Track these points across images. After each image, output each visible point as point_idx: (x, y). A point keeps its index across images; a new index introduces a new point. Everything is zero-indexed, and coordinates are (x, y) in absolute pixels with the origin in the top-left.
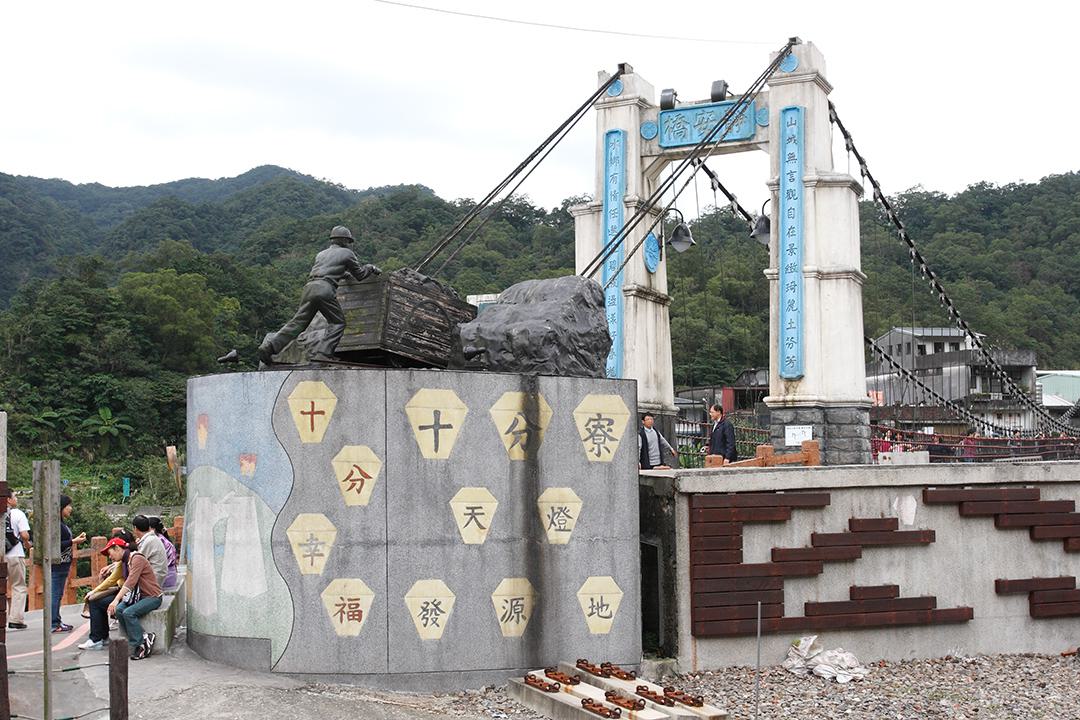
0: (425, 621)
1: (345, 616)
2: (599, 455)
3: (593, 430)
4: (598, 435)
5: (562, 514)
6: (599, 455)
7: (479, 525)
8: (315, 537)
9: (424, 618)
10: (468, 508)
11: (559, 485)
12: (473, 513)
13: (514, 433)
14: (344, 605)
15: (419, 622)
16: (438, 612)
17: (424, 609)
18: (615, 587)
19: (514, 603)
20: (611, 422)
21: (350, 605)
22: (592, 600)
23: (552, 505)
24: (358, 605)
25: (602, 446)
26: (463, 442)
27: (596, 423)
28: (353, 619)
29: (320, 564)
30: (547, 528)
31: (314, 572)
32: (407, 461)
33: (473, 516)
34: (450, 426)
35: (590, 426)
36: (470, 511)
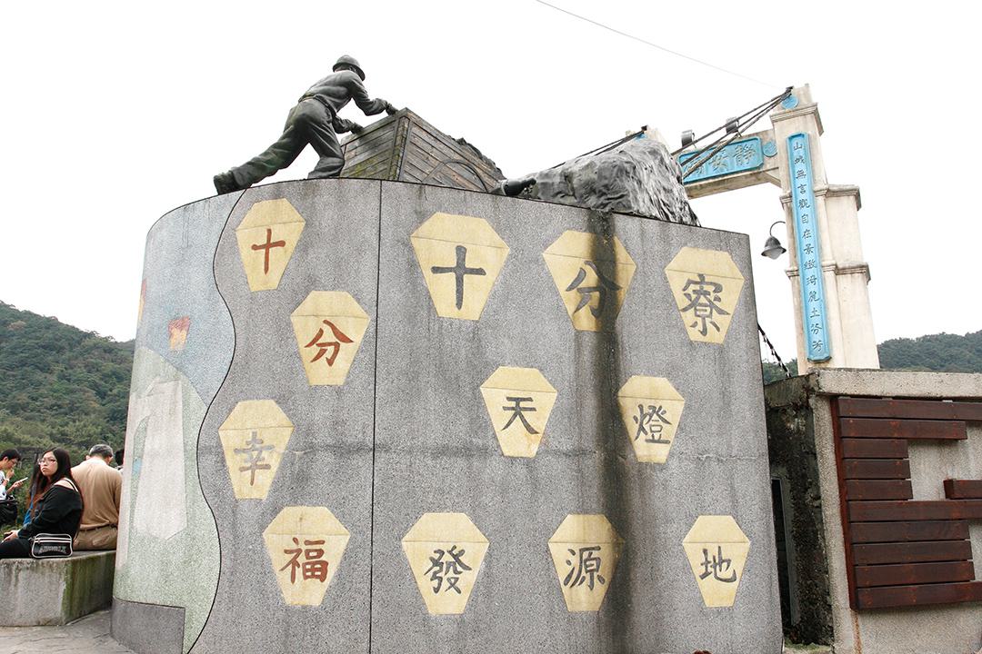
0: (436, 582)
1: (299, 571)
2: (704, 332)
3: (694, 296)
4: (701, 305)
5: (655, 417)
6: (704, 332)
7: (528, 427)
8: (258, 437)
9: (434, 577)
10: (510, 399)
11: (651, 372)
12: (518, 407)
13: (580, 290)
14: (299, 551)
15: (425, 585)
16: (459, 569)
17: (436, 563)
18: (738, 534)
19: (585, 555)
20: (718, 288)
21: (308, 552)
22: (705, 552)
23: (640, 401)
24: (321, 552)
25: (708, 320)
26: (502, 297)
27: (697, 287)
28: (313, 576)
29: (265, 479)
30: (633, 437)
31: (255, 495)
32: (411, 319)
33: (518, 412)
35: (690, 291)
36: (513, 404)
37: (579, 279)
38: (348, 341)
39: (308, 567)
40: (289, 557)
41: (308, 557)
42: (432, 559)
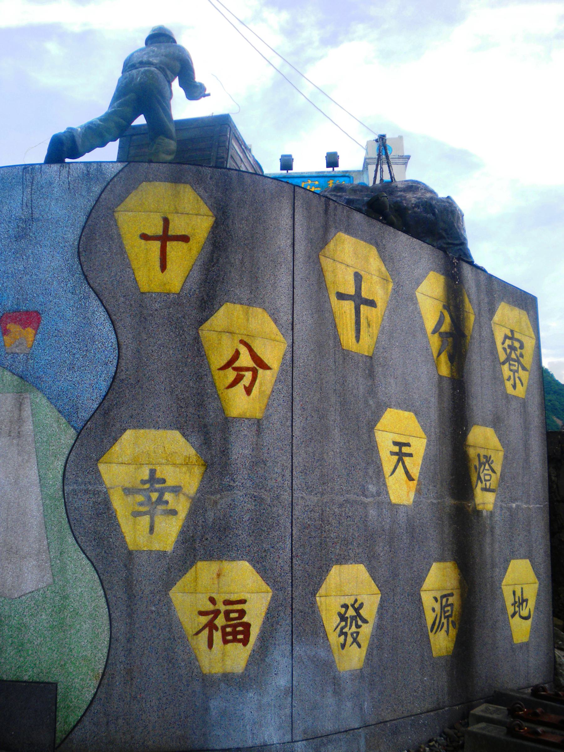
0: (343, 637)
1: (217, 636)
7: (407, 473)
8: (158, 475)
9: (342, 633)
11: (485, 424)
14: (216, 613)
15: (334, 639)
16: (360, 623)
17: (343, 618)
21: (227, 613)
24: (242, 613)
25: (516, 374)
28: (235, 640)
31: (156, 546)
32: (320, 346)
38: (266, 367)
39: (229, 630)
40: (204, 620)
41: (227, 618)
42: (339, 614)
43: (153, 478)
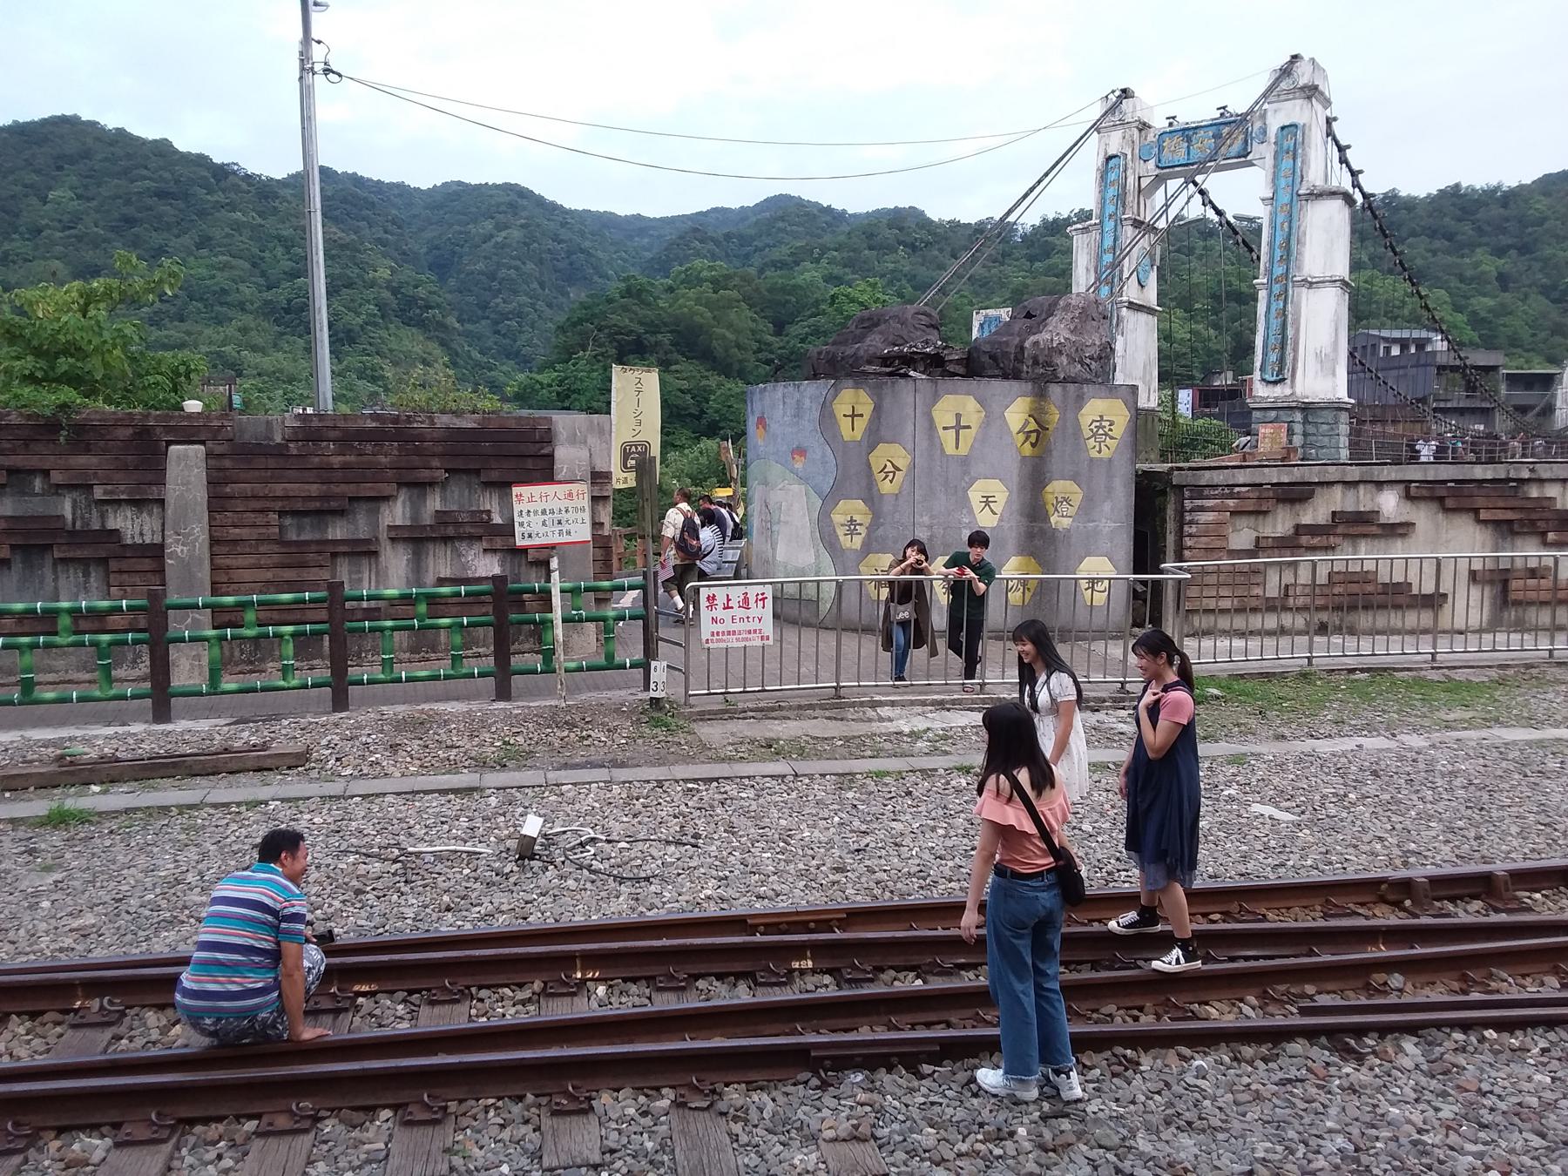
2: (1100, 452)
6: (1100, 452)
12: (987, 501)
26: (982, 439)
29: (857, 542)
33: (987, 503)
34: (969, 427)
37: (1025, 425)
38: (899, 470)
43: (852, 520)
